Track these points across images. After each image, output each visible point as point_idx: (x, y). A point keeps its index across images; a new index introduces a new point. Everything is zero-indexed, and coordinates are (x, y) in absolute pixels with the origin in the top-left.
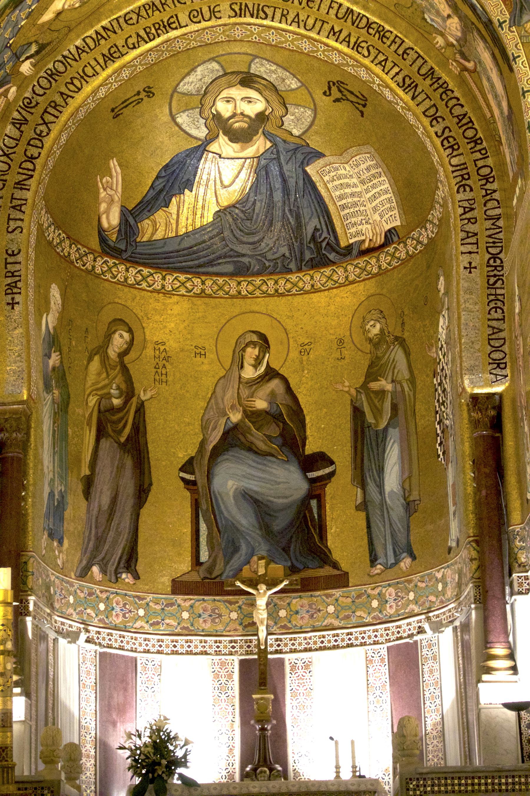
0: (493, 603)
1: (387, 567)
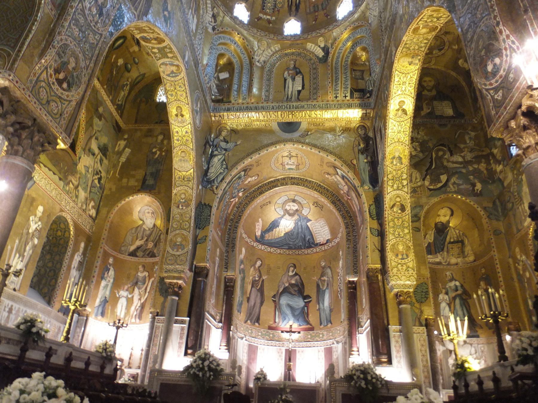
0: (354, 336)
1: (325, 326)
